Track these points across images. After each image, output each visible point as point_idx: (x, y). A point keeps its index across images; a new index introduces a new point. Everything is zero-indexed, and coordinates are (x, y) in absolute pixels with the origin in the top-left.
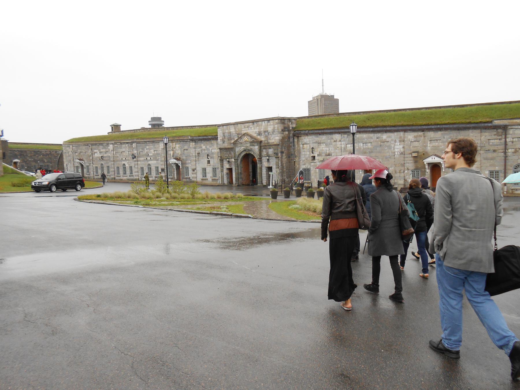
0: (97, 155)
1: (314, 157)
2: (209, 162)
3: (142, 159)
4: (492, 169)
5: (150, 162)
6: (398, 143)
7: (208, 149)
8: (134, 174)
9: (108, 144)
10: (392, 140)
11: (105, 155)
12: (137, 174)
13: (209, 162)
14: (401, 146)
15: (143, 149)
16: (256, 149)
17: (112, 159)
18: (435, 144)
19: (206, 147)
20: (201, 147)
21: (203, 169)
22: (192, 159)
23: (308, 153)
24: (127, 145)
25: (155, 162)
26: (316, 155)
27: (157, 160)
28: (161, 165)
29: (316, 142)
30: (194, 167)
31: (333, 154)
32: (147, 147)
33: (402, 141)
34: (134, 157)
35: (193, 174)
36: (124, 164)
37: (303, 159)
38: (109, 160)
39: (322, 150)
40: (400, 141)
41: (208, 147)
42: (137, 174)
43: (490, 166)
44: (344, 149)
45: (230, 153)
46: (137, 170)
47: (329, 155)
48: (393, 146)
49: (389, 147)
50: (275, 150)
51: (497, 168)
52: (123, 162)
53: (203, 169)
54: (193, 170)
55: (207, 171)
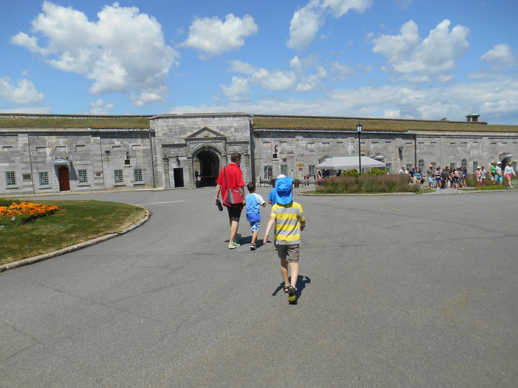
1: (275, 156)
2: (127, 162)
6: (350, 144)
7: (125, 146)
10: (345, 141)
13: (127, 162)
14: (353, 146)
16: (220, 145)
18: (376, 145)
19: (122, 143)
21: (116, 172)
22: (96, 158)
23: (269, 151)
25: (7, 164)
28: (23, 169)
29: (278, 141)
31: (295, 152)
35: (96, 179)
37: (264, 157)
39: (284, 148)
40: (352, 142)
43: (408, 161)
44: (306, 147)
47: (291, 153)
48: (346, 145)
49: (344, 147)
51: (410, 163)
53: (116, 172)
54: (98, 174)
55: (124, 174)
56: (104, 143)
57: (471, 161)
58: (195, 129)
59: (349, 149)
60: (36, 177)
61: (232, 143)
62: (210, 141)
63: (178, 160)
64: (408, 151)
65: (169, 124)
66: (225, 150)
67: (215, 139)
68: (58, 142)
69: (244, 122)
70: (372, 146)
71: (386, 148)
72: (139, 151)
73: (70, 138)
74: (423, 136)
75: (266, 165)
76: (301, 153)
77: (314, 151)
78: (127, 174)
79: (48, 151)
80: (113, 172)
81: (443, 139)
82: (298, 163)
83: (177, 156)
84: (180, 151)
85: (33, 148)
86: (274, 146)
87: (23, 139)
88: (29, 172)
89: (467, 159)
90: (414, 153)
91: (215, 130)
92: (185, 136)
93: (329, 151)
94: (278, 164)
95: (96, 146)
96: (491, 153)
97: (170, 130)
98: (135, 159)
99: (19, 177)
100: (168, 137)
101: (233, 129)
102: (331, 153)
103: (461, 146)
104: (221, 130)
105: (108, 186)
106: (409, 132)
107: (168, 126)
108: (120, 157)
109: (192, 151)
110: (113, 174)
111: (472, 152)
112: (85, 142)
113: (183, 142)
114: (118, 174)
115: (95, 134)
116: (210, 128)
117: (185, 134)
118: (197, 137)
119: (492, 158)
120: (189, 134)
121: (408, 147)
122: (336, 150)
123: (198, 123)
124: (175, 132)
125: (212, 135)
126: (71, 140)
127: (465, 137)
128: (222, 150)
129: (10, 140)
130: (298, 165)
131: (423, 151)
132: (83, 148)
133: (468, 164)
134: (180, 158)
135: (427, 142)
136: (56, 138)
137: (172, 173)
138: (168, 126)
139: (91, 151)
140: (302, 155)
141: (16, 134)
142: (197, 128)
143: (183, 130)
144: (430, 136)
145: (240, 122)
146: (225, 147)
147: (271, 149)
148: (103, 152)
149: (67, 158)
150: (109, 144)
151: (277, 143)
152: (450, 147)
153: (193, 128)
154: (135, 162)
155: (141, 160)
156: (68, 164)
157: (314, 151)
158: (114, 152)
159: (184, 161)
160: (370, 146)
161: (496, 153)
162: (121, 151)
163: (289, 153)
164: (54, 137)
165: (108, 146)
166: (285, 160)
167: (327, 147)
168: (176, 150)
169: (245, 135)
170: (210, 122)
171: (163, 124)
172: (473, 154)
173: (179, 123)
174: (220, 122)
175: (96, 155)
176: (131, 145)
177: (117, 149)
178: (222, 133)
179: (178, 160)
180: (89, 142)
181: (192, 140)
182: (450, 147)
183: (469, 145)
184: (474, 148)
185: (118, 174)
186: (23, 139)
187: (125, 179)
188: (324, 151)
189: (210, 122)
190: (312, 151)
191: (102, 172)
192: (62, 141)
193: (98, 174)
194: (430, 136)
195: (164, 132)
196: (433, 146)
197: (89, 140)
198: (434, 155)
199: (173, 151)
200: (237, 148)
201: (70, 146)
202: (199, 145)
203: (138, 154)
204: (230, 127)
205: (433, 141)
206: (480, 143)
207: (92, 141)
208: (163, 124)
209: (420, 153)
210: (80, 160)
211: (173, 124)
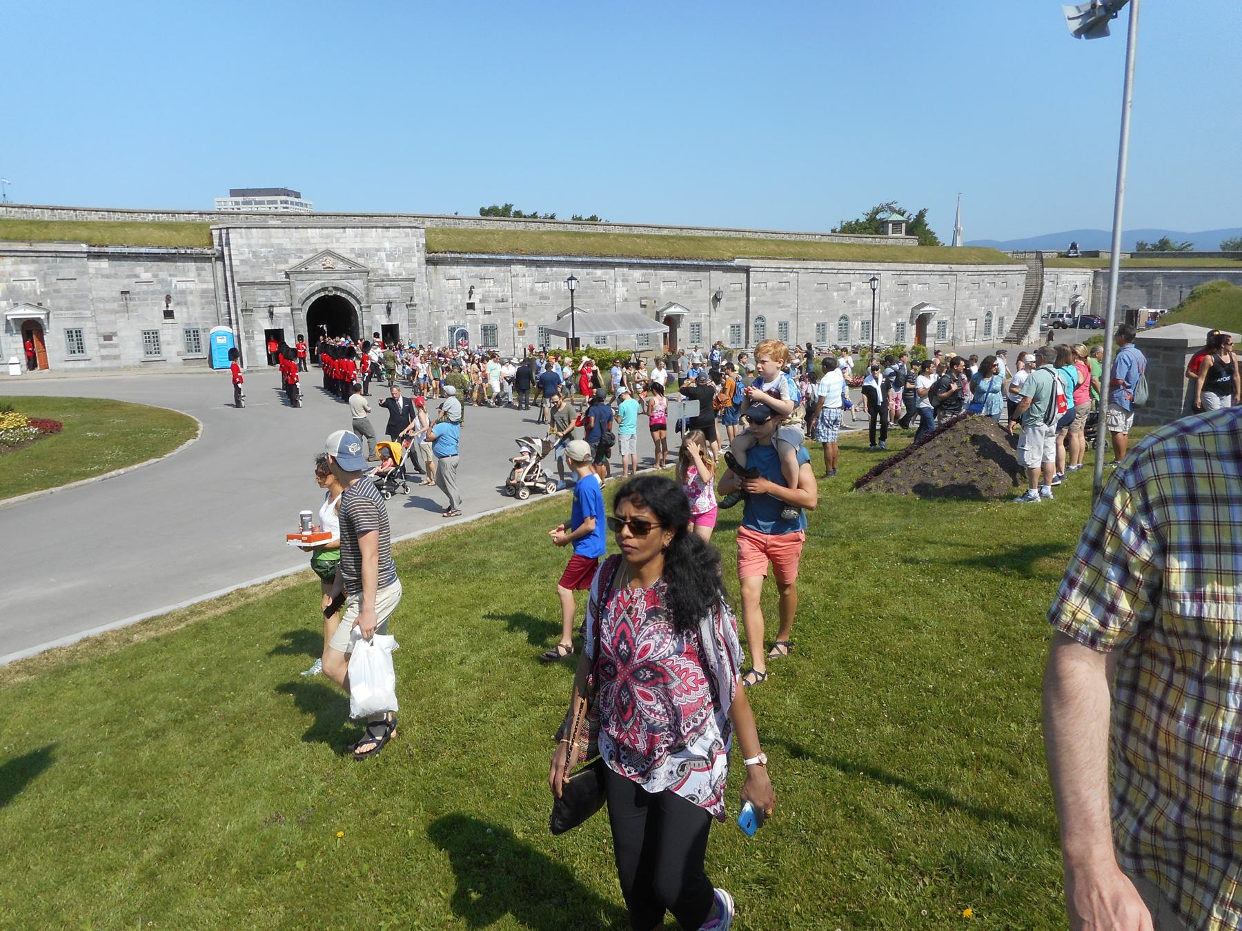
1: (471, 306)
2: (169, 314)
6: (619, 284)
7: (161, 282)
13: (169, 314)
16: (356, 286)
18: (671, 286)
19: (155, 276)
20: (137, 276)
22: (101, 306)
23: (459, 297)
26: (475, 299)
29: (476, 276)
30: (107, 330)
33: (625, 280)
41: (163, 275)
45: (276, 294)
48: (612, 287)
51: (738, 322)
55: (162, 338)
56: (116, 276)
58: (306, 253)
59: (618, 295)
61: (382, 280)
62: (337, 276)
63: (271, 314)
65: (253, 242)
66: (367, 295)
67: (347, 272)
68: (18, 271)
69: (405, 240)
70: (663, 288)
72: (191, 293)
73: (44, 264)
75: (452, 323)
76: (522, 300)
78: (169, 338)
80: (140, 333)
81: (803, 276)
82: (517, 320)
83: (271, 306)
84: (276, 294)
86: (468, 286)
89: (849, 315)
90: (744, 303)
91: (348, 256)
94: (477, 322)
95: (100, 280)
96: (896, 304)
97: (255, 254)
98: (185, 309)
100: (252, 267)
101: (383, 255)
104: (359, 256)
105: (131, 362)
106: (737, 262)
107: (249, 246)
108: (154, 304)
110: (140, 338)
112: (77, 273)
114: (151, 338)
116: (338, 251)
117: (287, 262)
118: (311, 268)
119: (899, 313)
120: (294, 261)
122: (592, 297)
123: (312, 241)
124: (265, 257)
126: (45, 266)
128: (361, 295)
130: (515, 325)
132: (74, 284)
134: (276, 310)
135: (773, 281)
136: (14, 263)
138: (249, 246)
139: (90, 290)
140: (524, 307)
142: (311, 251)
145: (398, 240)
146: (367, 289)
147: (463, 293)
148: (119, 295)
149: (40, 304)
150: (128, 277)
151: (474, 282)
152: (817, 290)
153: (301, 251)
154: (185, 315)
155: (196, 312)
156: (42, 317)
158: (139, 293)
159: (286, 315)
161: (907, 304)
162: (153, 293)
163: (498, 301)
164: (8, 261)
165: (126, 281)
168: (269, 293)
169: (407, 265)
170: (337, 241)
171: (241, 241)
173: (275, 241)
174: (358, 240)
175: (103, 300)
176: (174, 280)
177: (144, 287)
178: (361, 261)
179: (271, 314)
180: (85, 273)
181: (301, 273)
182: (817, 290)
185: (151, 338)
187: (163, 348)
189: (337, 241)
190: (544, 297)
191: (115, 334)
192: (26, 269)
193: (108, 338)
195: (241, 257)
196: (784, 289)
197: (86, 267)
199: (262, 296)
200: (392, 291)
201: (44, 279)
202: (317, 284)
203: (190, 298)
204: (378, 250)
205: (785, 279)
207: (91, 271)
208: (241, 241)
209: (756, 303)
210: (68, 309)
211: (261, 241)
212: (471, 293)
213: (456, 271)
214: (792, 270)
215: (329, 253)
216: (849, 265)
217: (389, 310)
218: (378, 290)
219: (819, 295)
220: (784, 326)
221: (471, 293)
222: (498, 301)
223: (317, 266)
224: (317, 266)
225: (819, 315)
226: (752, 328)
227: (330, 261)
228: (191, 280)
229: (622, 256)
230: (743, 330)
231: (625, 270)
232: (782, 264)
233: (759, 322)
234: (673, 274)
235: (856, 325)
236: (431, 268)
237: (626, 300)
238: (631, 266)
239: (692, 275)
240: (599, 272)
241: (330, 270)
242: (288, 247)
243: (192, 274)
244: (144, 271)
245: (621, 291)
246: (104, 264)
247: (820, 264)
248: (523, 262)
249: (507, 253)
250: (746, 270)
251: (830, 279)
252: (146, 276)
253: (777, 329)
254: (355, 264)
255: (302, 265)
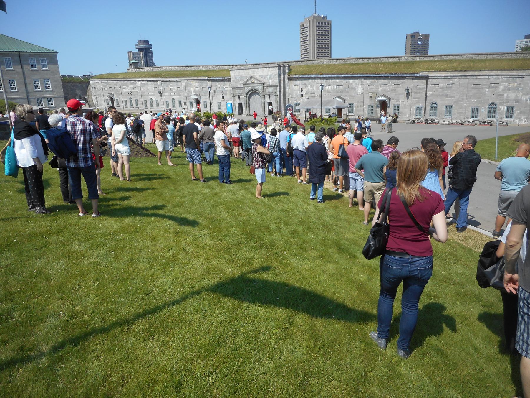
0: (126, 90)
1: (302, 96)
2: (223, 97)
3: (166, 94)
4: (418, 105)
5: (174, 97)
6: (360, 86)
7: (222, 88)
8: (160, 106)
9: (135, 82)
11: (133, 91)
12: (163, 106)
13: (223, 97)
15: (167, 86)
17: (140, 94)
18: (384, 87)
21: (218, 103)
24: (153, 82)
25: (179, 97)
26: (304, 93)
27: (180, 95)
32: (171, 85)
33: (363, 85)
34: (160, 93)
36: (151, 99)
38: (137, 95)
41: (222, 86)
42: (163, 106)
43: (417, 103)
46: (162, 103)
49: (354, 89)
50: (274, 89)
51: (421, 105)
52: (150, 97)
53: (218, 103)
57: (503, 105)
59: (359, 91)
60: (188, 104)
62: (255, 85)
63: (239, 98)
64: (419, 93)
66: (263, 91)
67: (257, 83)
70: (380, 88)
71: (395, 90)
74: (437, 77)
77: (330, 92)
79: (192, 90)
81: (463, 81)
85: (187, 88)
87: (183, 83)
88: (186, 101)
89: (497, 102)
92: (242, 82)
93: (342, 92)
99: (183, 103)
101: (268, 77)
102: (344, 94)
103: (489, 88)
104: (262, 78)
106: (422, 74)
109: (246, 92)
110: (217, 104)
111: (505, 95)
113: (242, 86)
115: (209, 80)
118: (248, 82)
120: (245, 80)
121: (420, 89)
122: (348, 92)
125: (256, 82)
127: (497, 77)
129: (179, 83)
131: (437, 93)
133: (497, 109)
135: (443, 83)
137: (237, 105)
141: (180, 81)
143: (242, 78)
144: (446, 77)
151: (303, 86)
152: (473, 88)
153: (247, 77)
157: (330, 92)
160: (378, 88)
163: (311, 94)
166: (308, 98)
167: (339, 90)
169: (275, 81)
172: (507, 97)
173: (241, 74)
177: (218, 89)
179: (239, 98)
182: (473, 88)
183: (502, 87)
184: (509, 90)
186: (183, 83)
188: (338, 92)
194: (446, 77)
196: (451, 88)
198: (449, 97)
199: (238, 92)
200: (270, 90)
205: (451, 82)
206: (520, 84)
209: (432, 95)
212: (302, 91)
213: (297, 82)
214: (456, 77)
215: (252, 77)
216: (499, 73)
217: (270, 97)
218: (267, 90)
219: (474, 91)
220: (449, 108)
221: (302, 91)
222: (311, 94)
223: (250, 82)
224: (250, 82)
225: (474, 102)
226: (428, 108)
227: (253, 80)
228: (227, 87)
229: (362, 74)
230: (423, 109)
231: (363, 80)
232: (450, 74)
233: (434, 105)
234: (386, 81)
235: (503, 109)
236: (289, 82)
237: (362, 93)
238: (365, 78)
239: (396, 82)
240: (351, 82)
241: (253, 83)
242: (244, 75)
243: (228, 85)
244: (218, 84)
245: (360, 89)
246: (210, 82)
247: (476, 73)
248: (320, 78)
249: (316, 74)
250: (426, 78)
251: (484, 82)
252: (219, 86)
253: (444, 109)
254: (259, 81)
255: (246, 81)
